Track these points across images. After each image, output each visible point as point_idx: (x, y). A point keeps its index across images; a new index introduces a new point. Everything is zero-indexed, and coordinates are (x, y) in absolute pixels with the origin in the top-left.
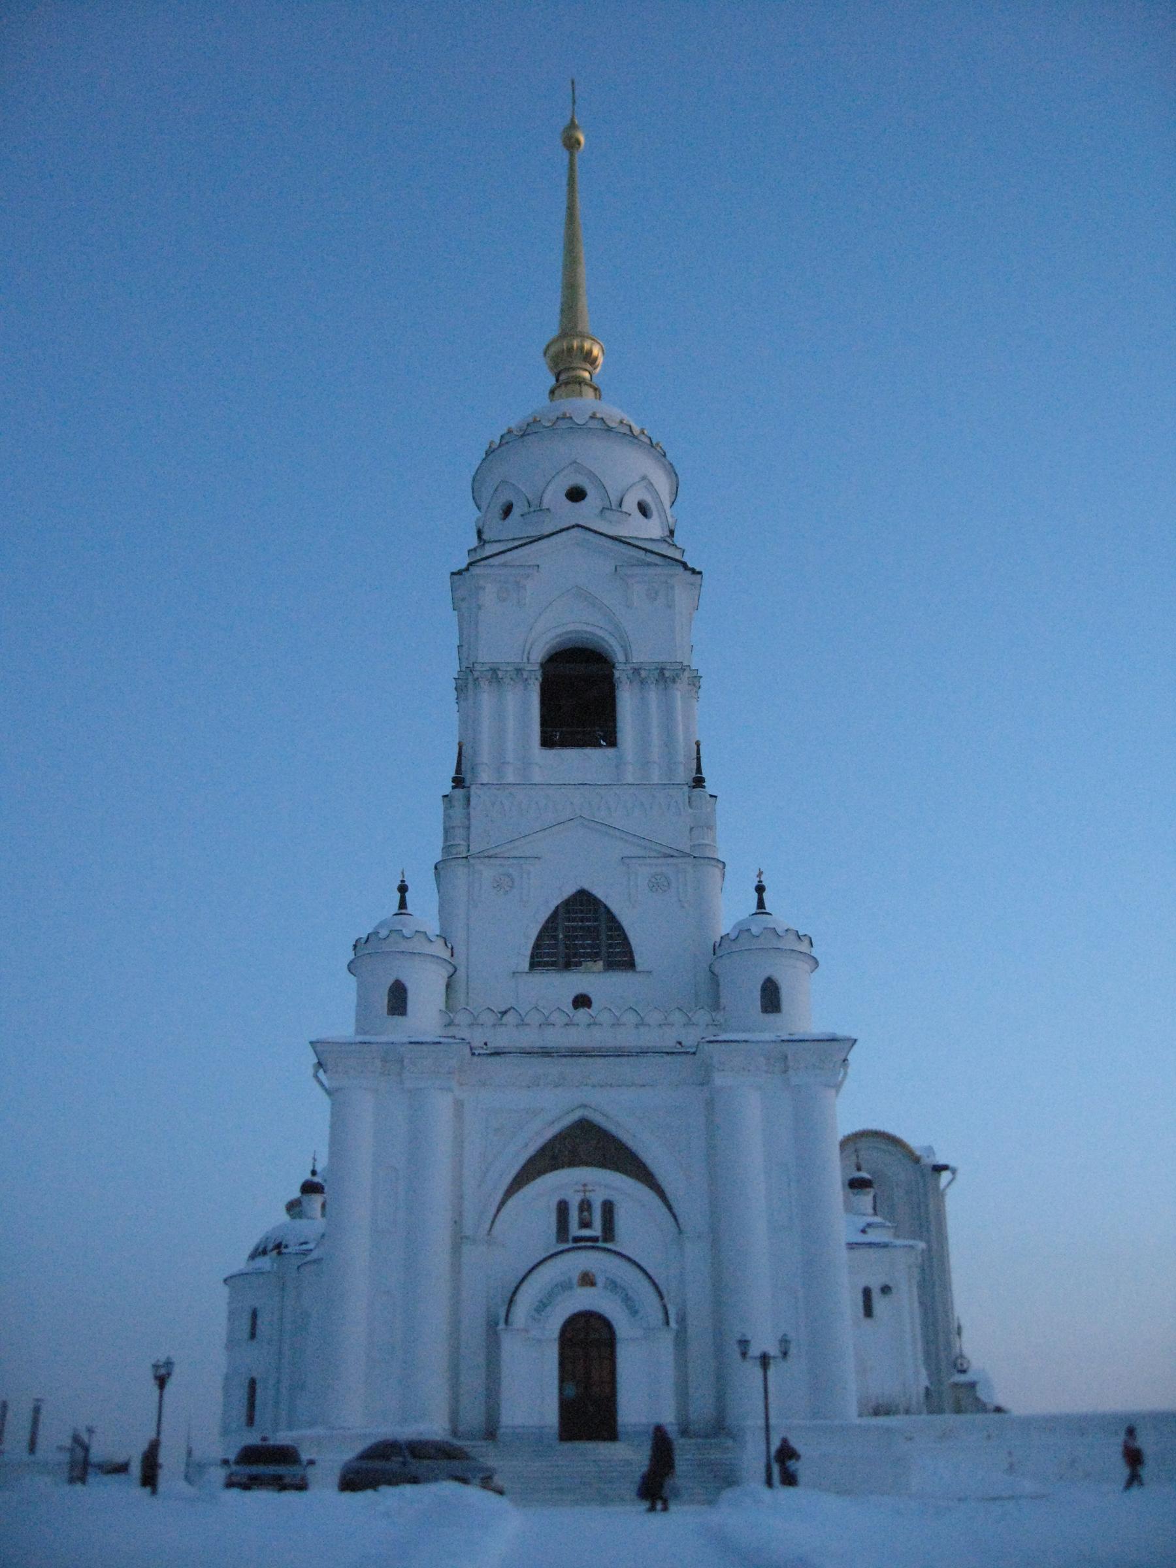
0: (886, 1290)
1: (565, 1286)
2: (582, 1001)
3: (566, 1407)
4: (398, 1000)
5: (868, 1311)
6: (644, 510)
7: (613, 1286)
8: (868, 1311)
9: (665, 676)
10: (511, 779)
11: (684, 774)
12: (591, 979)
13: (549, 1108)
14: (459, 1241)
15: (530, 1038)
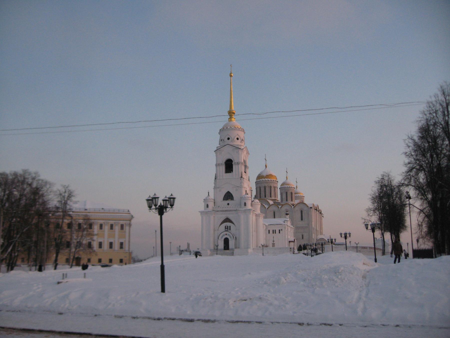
0: (282, 230)
1: (224, 235)
2: (228, 204)
3: (224, 247)
4: (207, 206)
5: (279, 233)
6: (238, 139)
7: (229, 235)
8: (279, 233)
9: (238, 164)
10: (221, 178)
11: (240, 176)
12: (229, 201)
13: (223, 216)
14: (214, 230)
15: (221, 209)
